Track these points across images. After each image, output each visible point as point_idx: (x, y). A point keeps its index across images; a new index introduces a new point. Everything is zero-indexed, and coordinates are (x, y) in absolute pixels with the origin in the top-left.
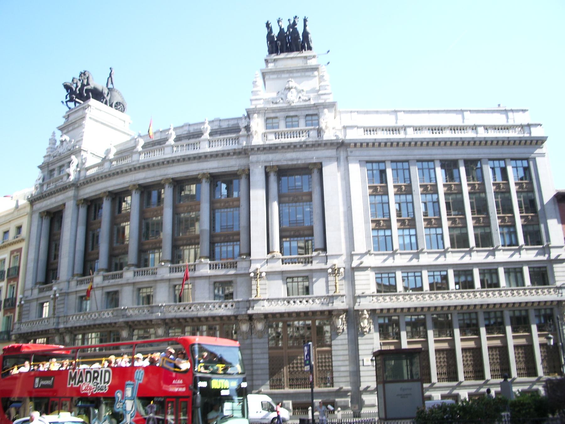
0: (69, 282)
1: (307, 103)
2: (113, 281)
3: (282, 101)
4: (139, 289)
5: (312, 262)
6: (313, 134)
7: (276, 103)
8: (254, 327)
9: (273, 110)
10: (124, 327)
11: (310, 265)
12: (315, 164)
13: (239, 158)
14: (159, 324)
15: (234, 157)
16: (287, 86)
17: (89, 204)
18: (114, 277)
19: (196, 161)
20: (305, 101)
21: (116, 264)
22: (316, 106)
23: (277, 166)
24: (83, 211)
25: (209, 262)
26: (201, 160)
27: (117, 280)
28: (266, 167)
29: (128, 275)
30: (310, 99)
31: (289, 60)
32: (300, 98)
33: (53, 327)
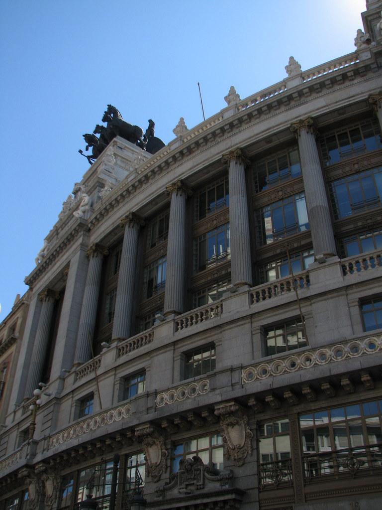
0: (64, 379)
2: (136, 351)
4: (188, 355)
10: (150, 435)
13: (366, 81)
14: (231, 413)
15: (355, 81)
17: (106, 252)
18: (137, 344)
19: (283, 108)
21: (141, 320)
24: (94, 264)
25: (339, 260)
26: (292, 103)
27: (142, 348)
29: (164, 332)
33: (23, 462)
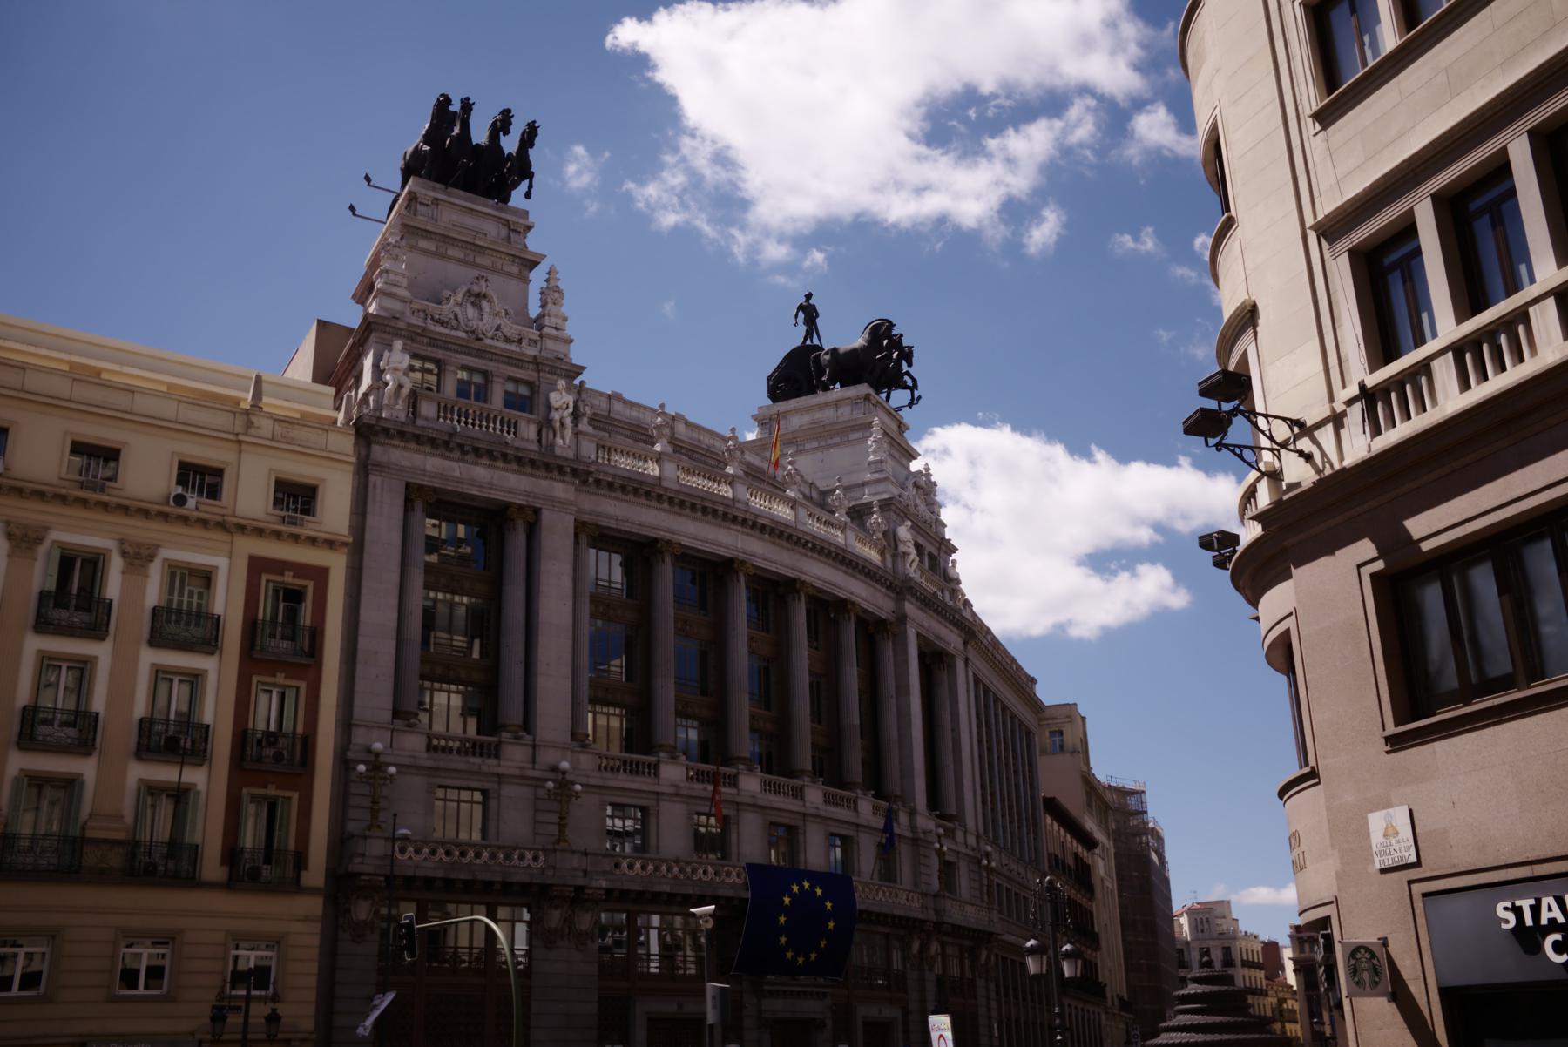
1: (513, 347)
3: (454, 323)
5: (497, 756)
6: (529, 431)
7: (442, 324)
8: (349, 911)
9: (435, 341)
11: (492, 761)
12: (521, 508)
16: (476, 289)
20: (507, 340)
22: (537, 363)
23: (435, 490)
28: (408, 485)
30: (520, 341)
31: (458, 212)
32: (498, 329)
